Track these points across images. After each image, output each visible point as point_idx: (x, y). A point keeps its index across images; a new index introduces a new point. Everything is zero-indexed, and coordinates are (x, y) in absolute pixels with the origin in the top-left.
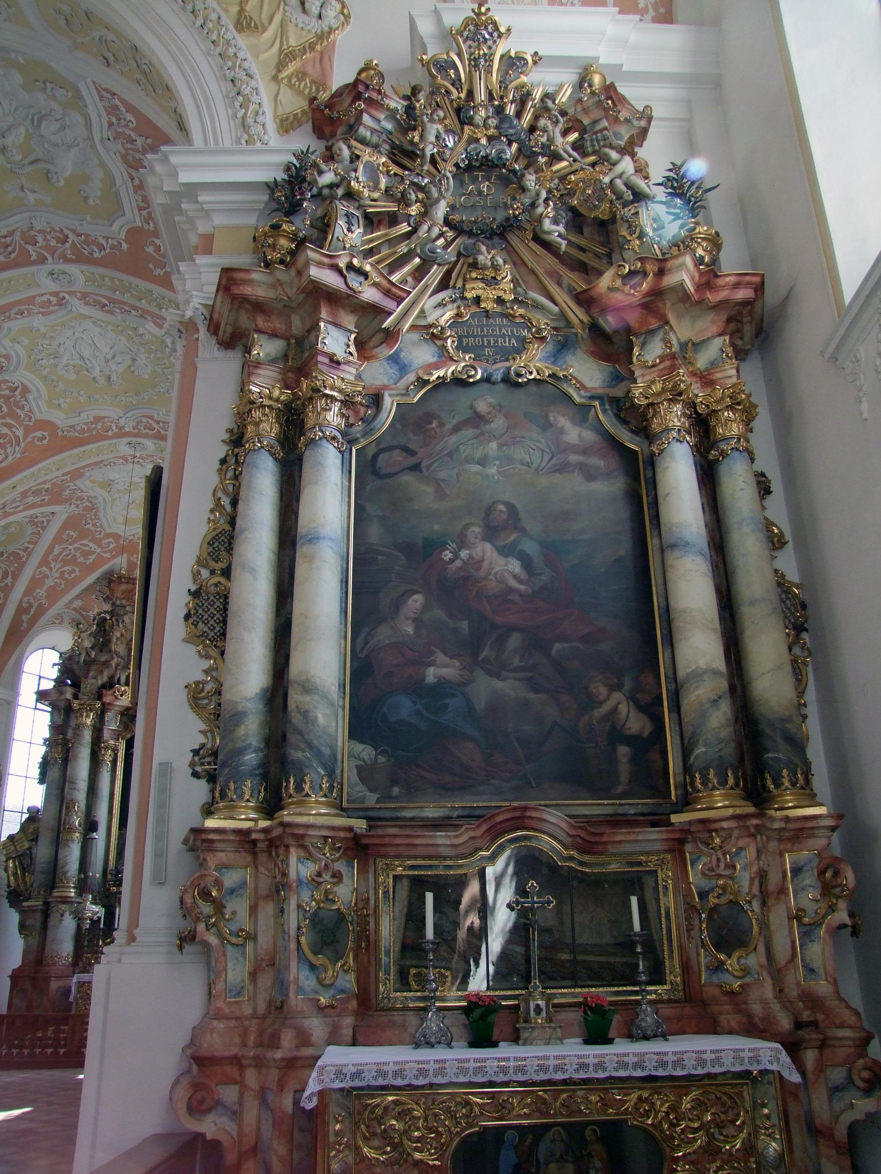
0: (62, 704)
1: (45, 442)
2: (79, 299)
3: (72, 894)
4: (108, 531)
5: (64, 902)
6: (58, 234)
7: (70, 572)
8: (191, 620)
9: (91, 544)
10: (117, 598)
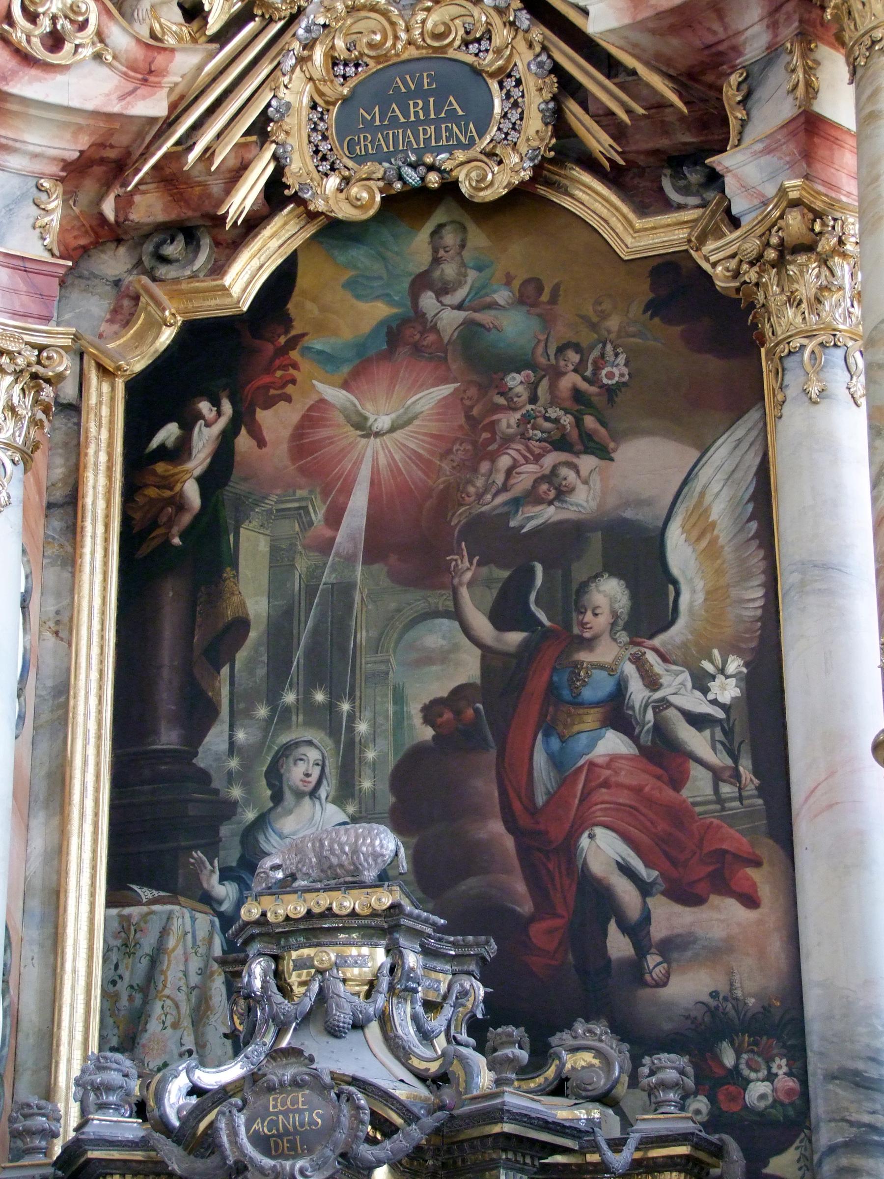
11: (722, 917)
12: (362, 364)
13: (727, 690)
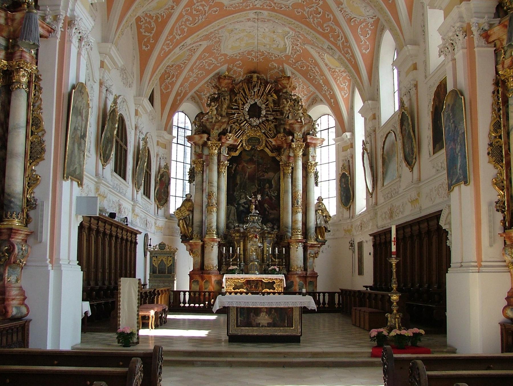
0: (201, 142)
1: (217, 13)
3: (215, 237)
4: (223, 52)
5: (213, 241)
7: (201, 74)
8: (490, 155)
9: (213, 60)
10: (222, 87)
11: (275, 212)
12: (248, 162)
13: (276, 194)
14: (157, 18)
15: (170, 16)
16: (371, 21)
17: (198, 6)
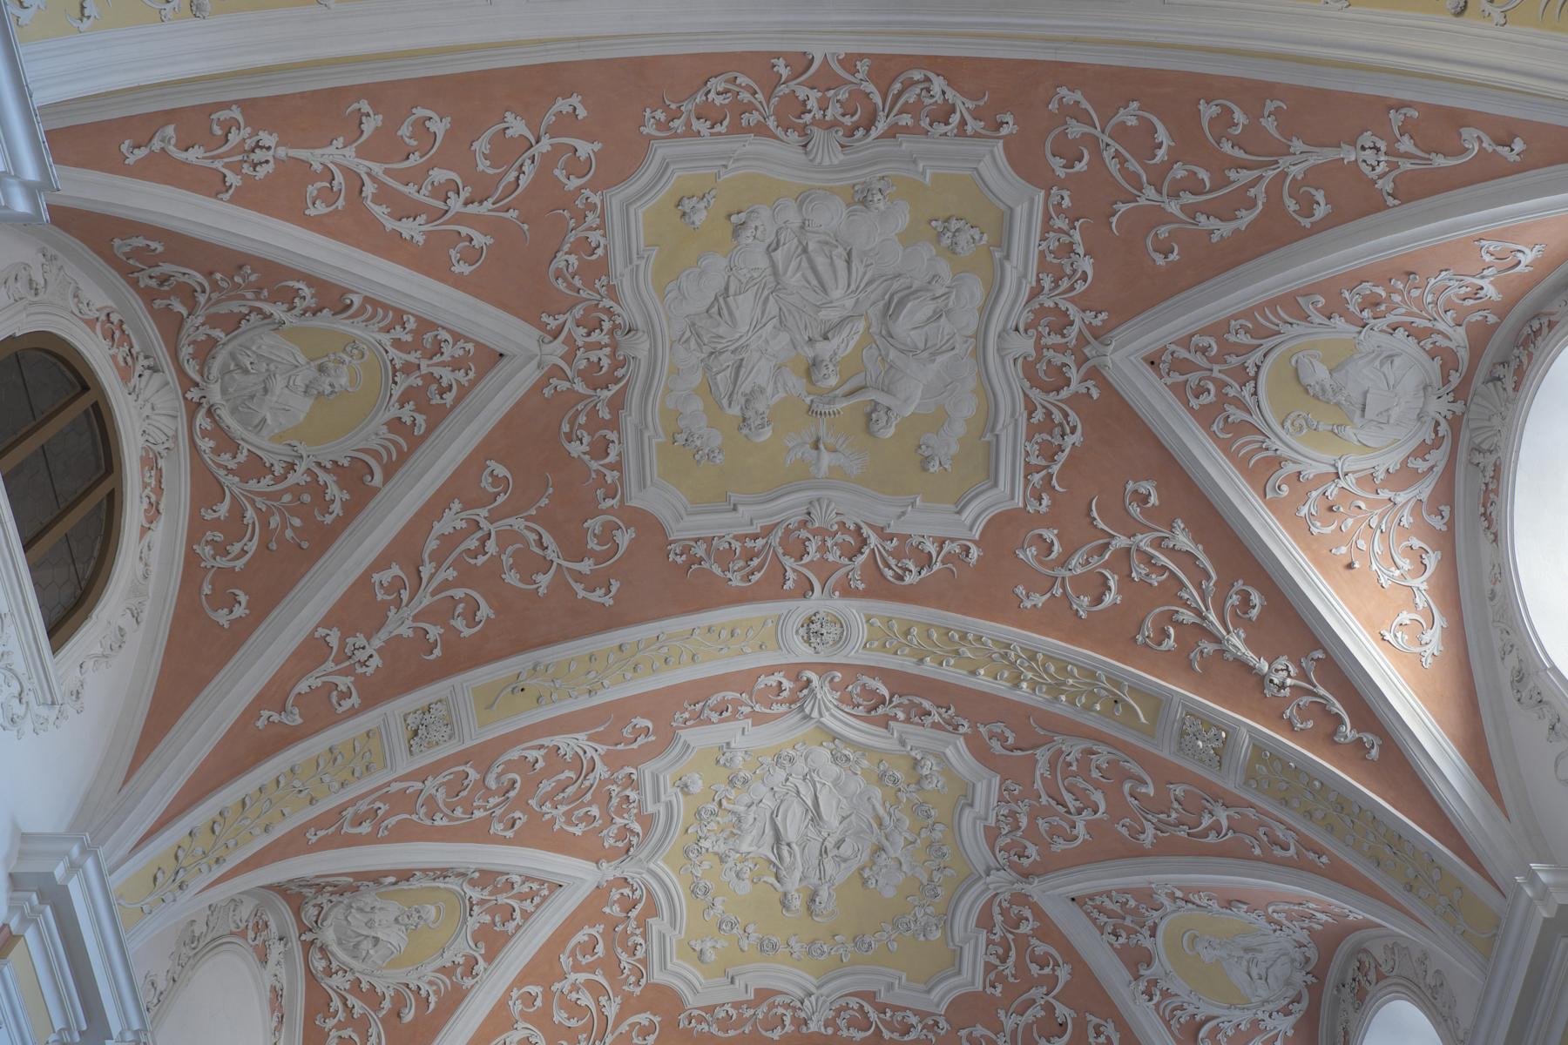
2: (834, 688)
6: (848, 538)
14: (399, 1002)
15: (453, 1000)
16: (1285, 1025)
17: (575, 988)
